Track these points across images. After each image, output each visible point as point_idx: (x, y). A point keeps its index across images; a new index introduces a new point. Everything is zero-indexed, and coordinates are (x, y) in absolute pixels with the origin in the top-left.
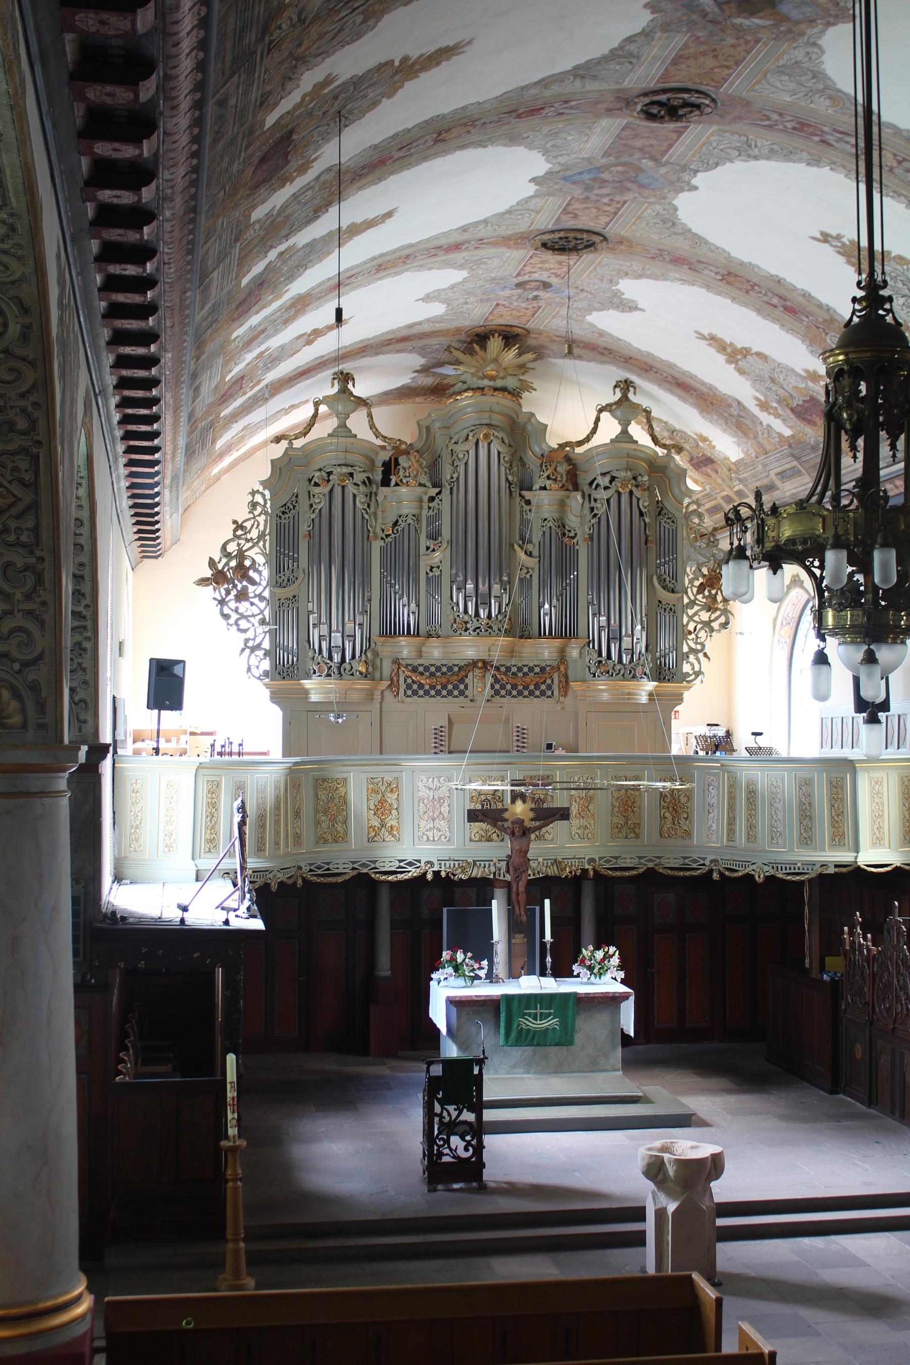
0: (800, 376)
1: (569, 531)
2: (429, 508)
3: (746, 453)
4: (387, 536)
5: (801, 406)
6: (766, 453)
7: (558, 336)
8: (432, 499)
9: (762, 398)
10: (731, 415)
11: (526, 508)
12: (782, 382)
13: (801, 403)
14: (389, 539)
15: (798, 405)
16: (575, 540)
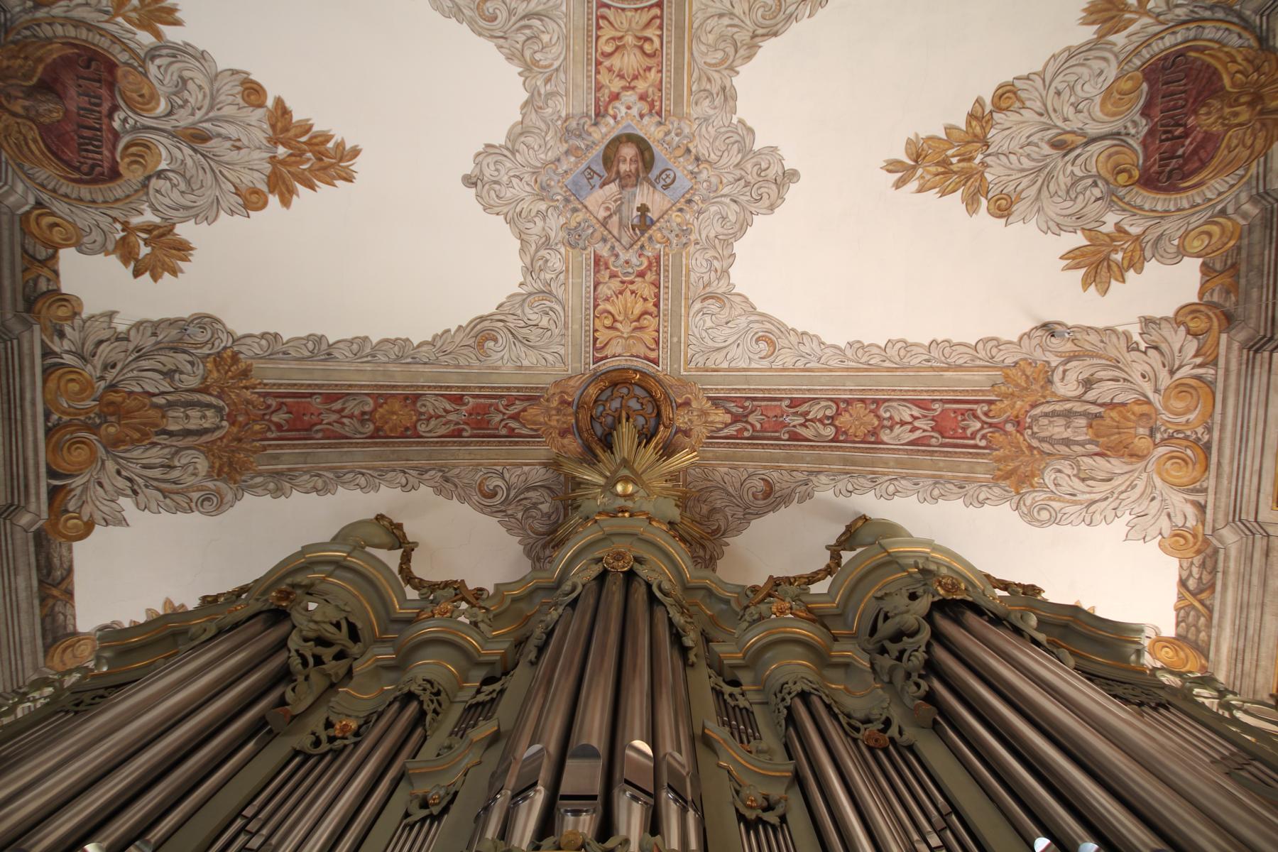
0: (1092, 46)
1: (867, 721)
2: (479, 692)
3: (1176, 541)
4: (332, 739)
5: (1151, 133)
6: (1207, 448)
7: (716, 402)
8: (488, 681)
9: (1079, 240)
10: (1068, 415)
11: (727, 689)
12: (1075, 124)
13: (1144, 126)
14: (338, 744)
15: (1144, 144)
16: (893, 731)
